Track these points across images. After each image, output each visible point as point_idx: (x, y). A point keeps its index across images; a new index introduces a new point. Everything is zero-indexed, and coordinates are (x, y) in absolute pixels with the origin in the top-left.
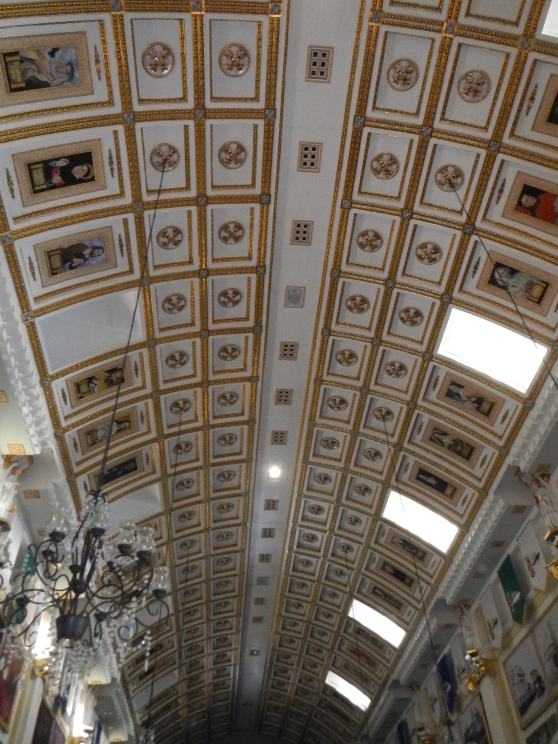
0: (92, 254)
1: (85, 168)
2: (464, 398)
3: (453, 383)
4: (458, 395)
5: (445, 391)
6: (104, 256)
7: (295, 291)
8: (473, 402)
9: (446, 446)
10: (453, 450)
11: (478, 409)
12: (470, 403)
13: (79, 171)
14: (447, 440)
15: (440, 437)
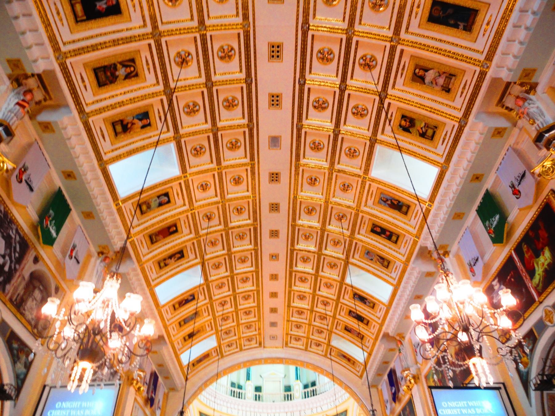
0: (387, 200)
1: (375, 229)
2: (136, 121)
3: (149, 125)
4: (140, 120)
5: (151, 114)
6: (382, 196)
7: (275, 146)
8: (128, 123)
9: (119, 65)
10: (111, 66)
11: (122, 121)
12: (130, 121)
13: (379, 230)
14: (121, 72)
15: (128, 70)
